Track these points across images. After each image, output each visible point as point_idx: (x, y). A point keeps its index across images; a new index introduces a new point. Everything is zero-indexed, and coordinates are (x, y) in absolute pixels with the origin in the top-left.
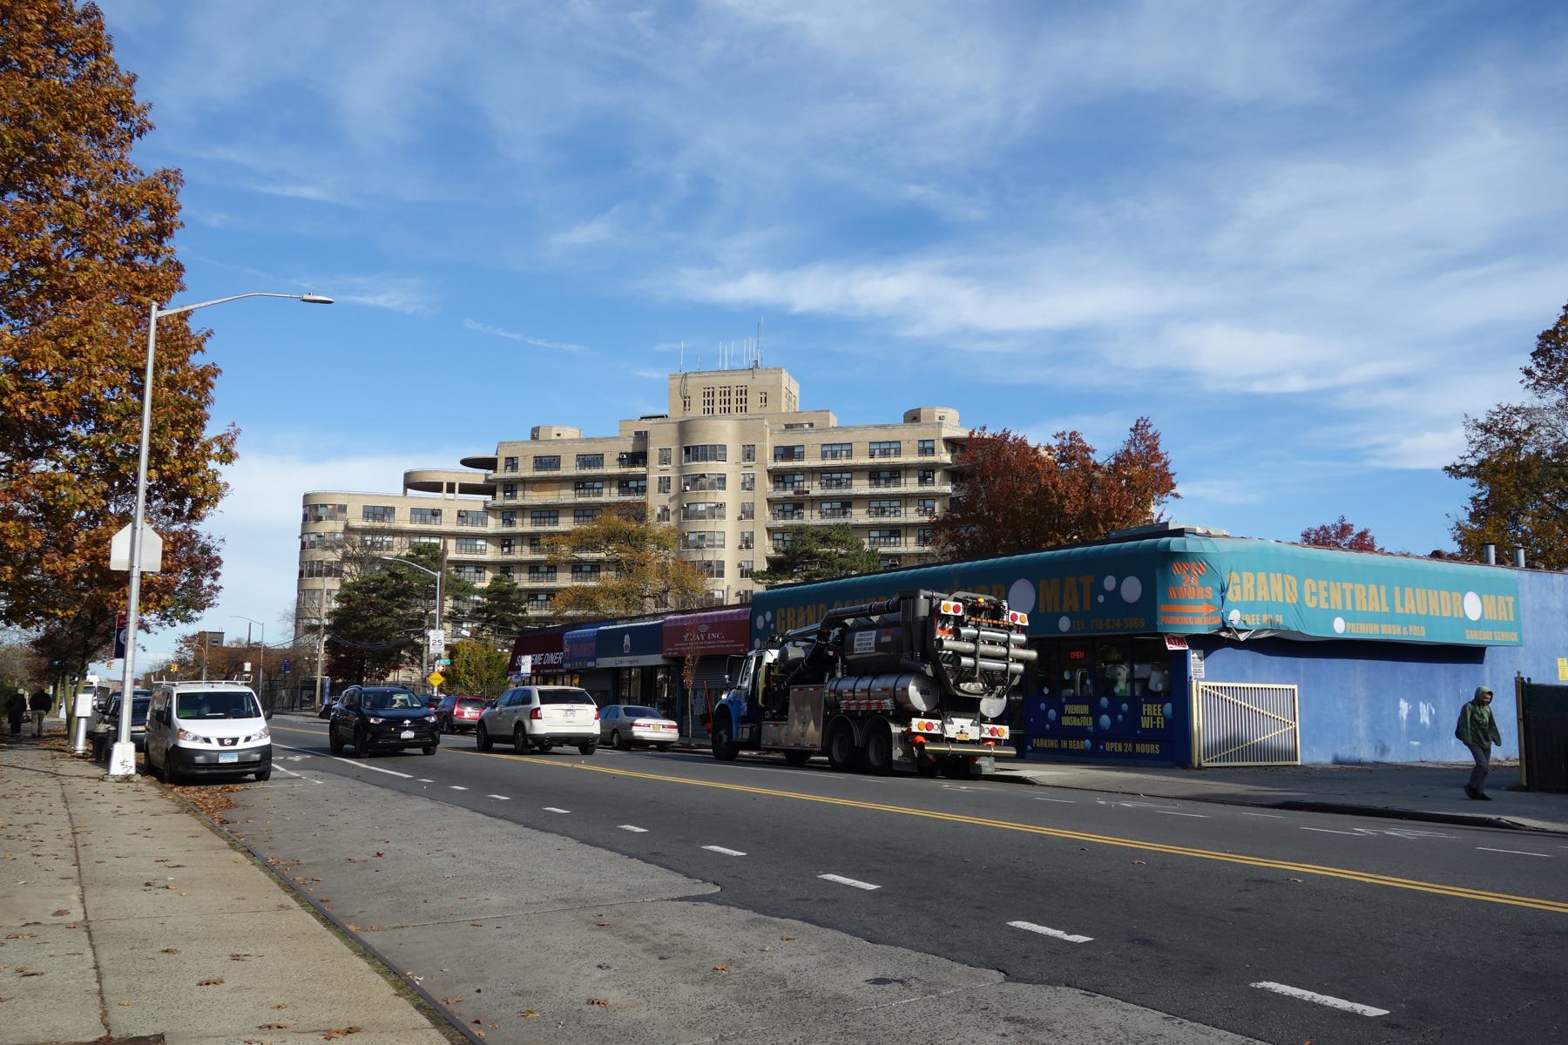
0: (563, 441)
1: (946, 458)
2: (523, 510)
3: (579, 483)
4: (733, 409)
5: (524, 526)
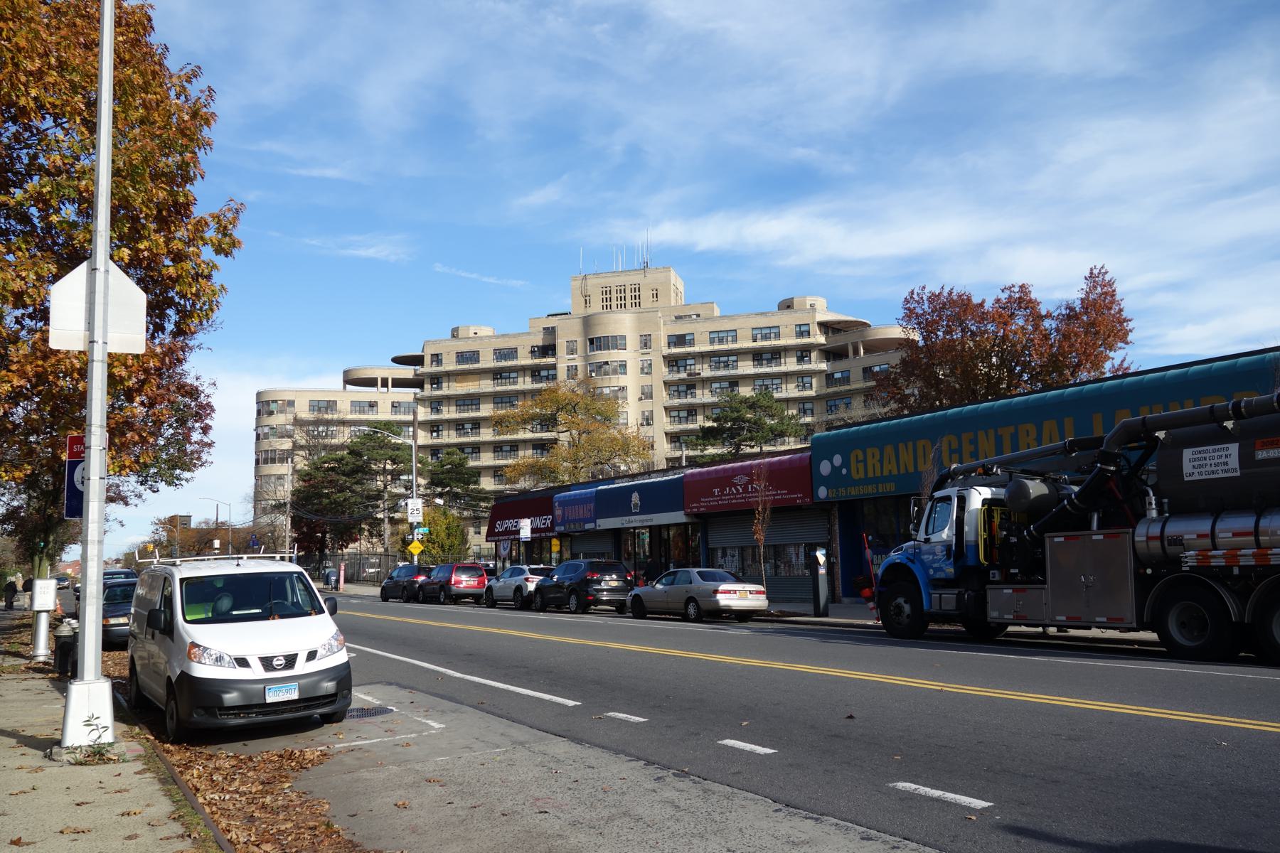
0: (481, 338)
1: (821, 339)
2: (448, 399)
3: (497, 374)
4: (628, 305)
5: (450, 413)
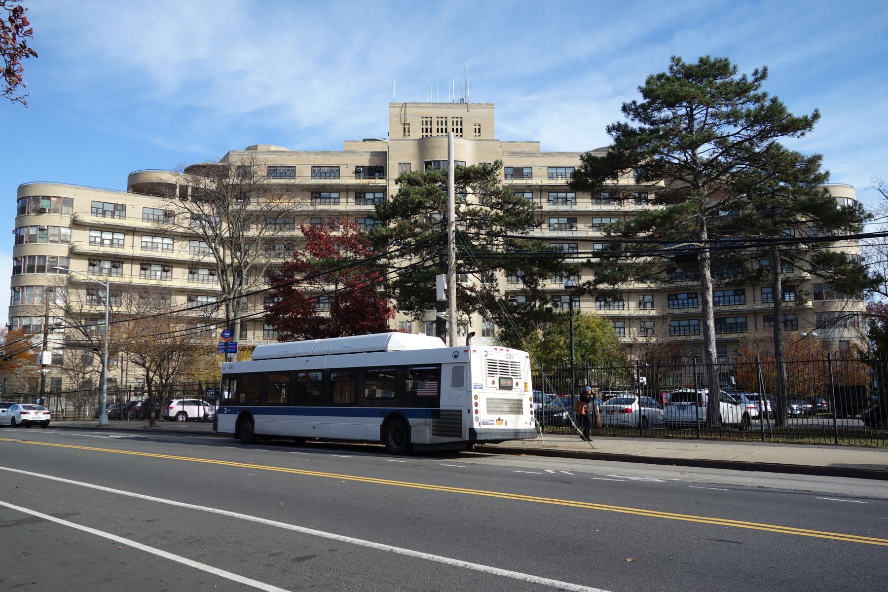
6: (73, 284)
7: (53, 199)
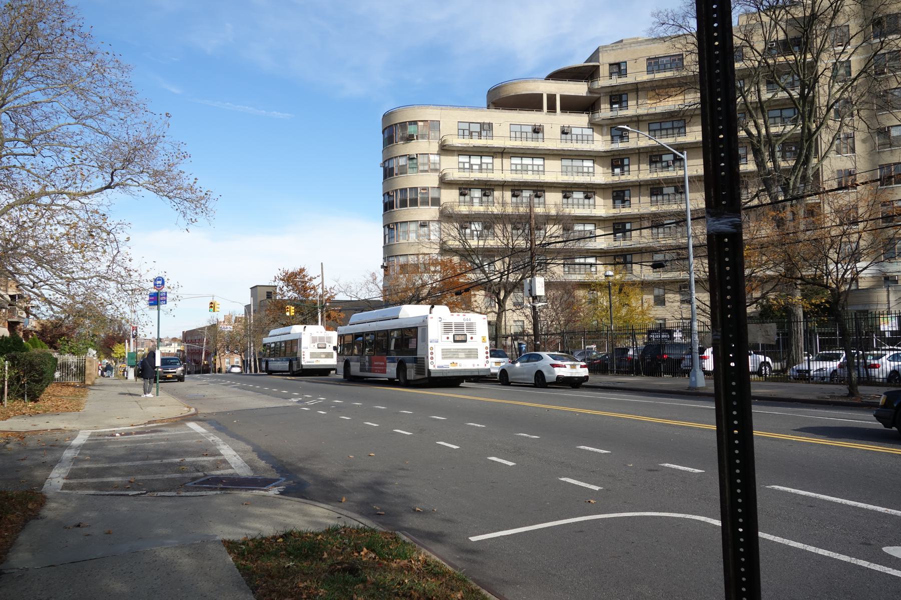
2: (636, 121)
5: (640, 140)
6: (446, 216)
7: (420, 124)
